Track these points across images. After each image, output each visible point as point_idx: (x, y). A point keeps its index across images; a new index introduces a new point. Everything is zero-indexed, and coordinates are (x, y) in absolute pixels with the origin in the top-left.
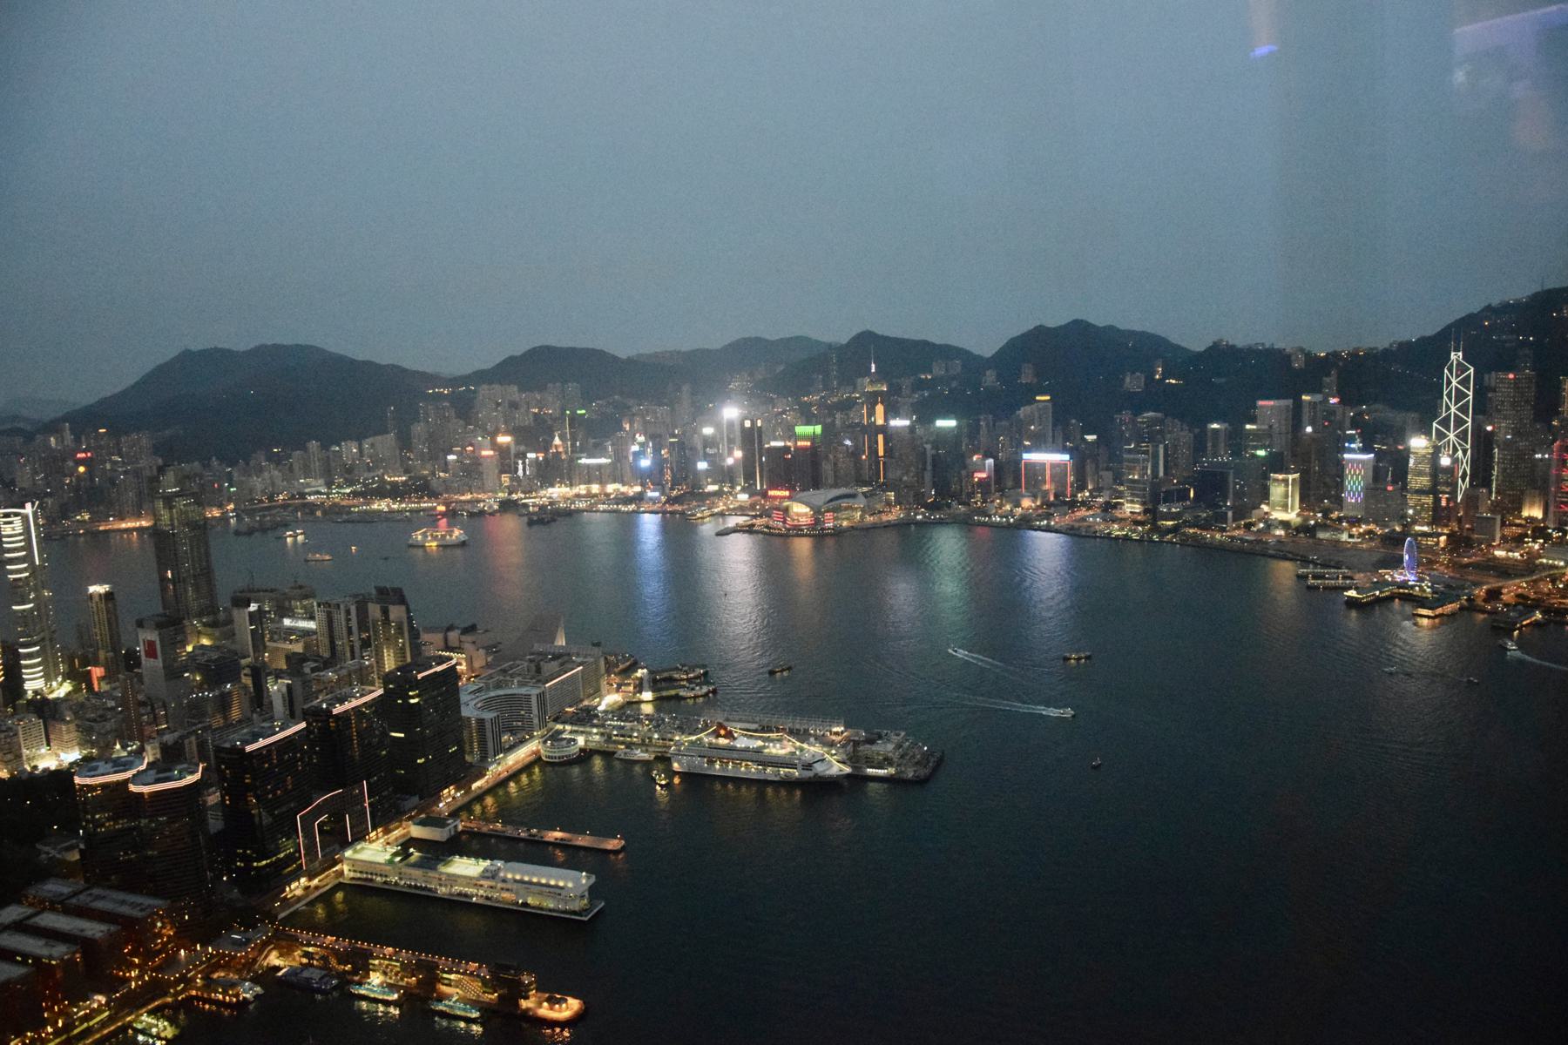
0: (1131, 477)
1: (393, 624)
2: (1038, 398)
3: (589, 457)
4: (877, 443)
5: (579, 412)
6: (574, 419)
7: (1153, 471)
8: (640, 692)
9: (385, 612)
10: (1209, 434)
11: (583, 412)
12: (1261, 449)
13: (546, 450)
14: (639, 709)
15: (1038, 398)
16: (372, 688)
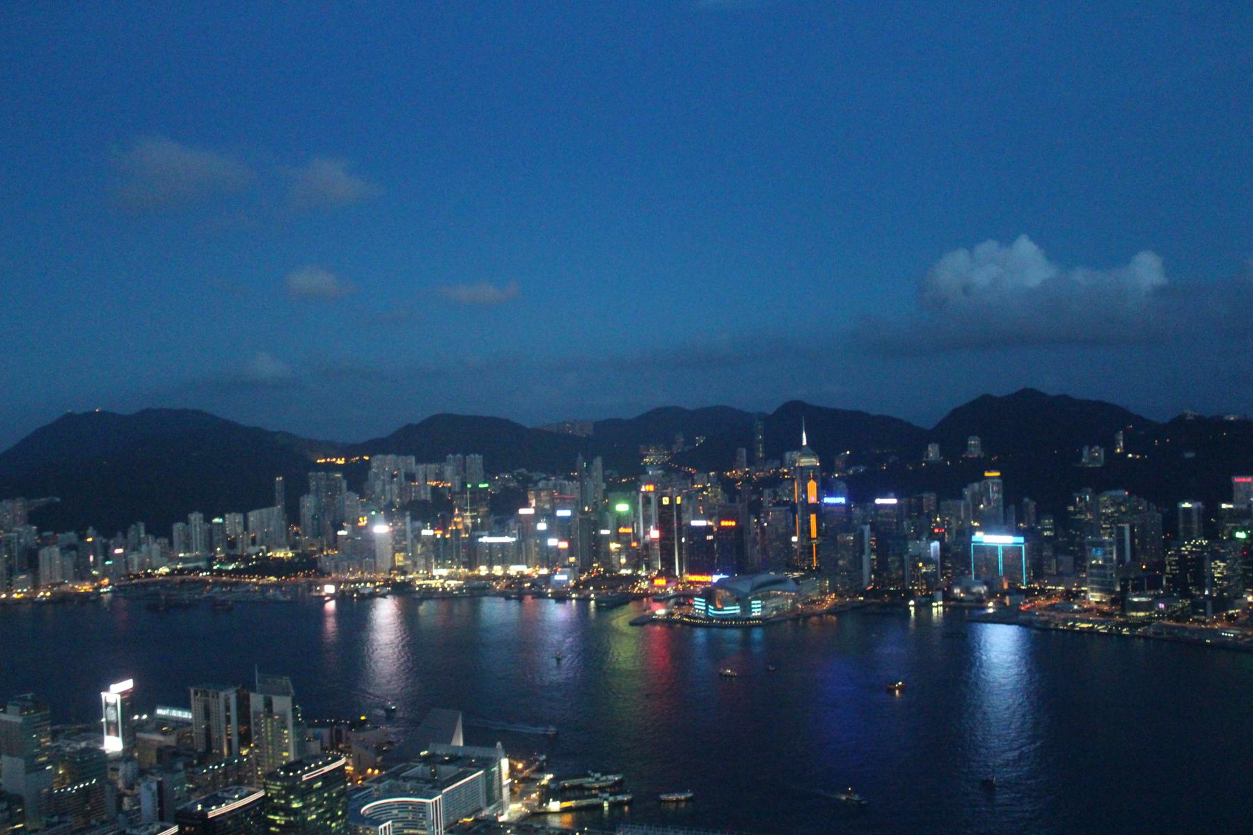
0: (1093, 562)
1: (276, 717)
2: (987, 474)
3: (491, 535)
4: (808, 522)
5: (481, 486)
6: (477, 493)
7: (1118, 556)
8: (548, 803)
9: (269, 704)
10: (1181, 515)
11: (486, 485)
12: (1241, 531)
13: (444, 528)
14: (545, 822)
15: (987, 474)
16: (252, 789)
